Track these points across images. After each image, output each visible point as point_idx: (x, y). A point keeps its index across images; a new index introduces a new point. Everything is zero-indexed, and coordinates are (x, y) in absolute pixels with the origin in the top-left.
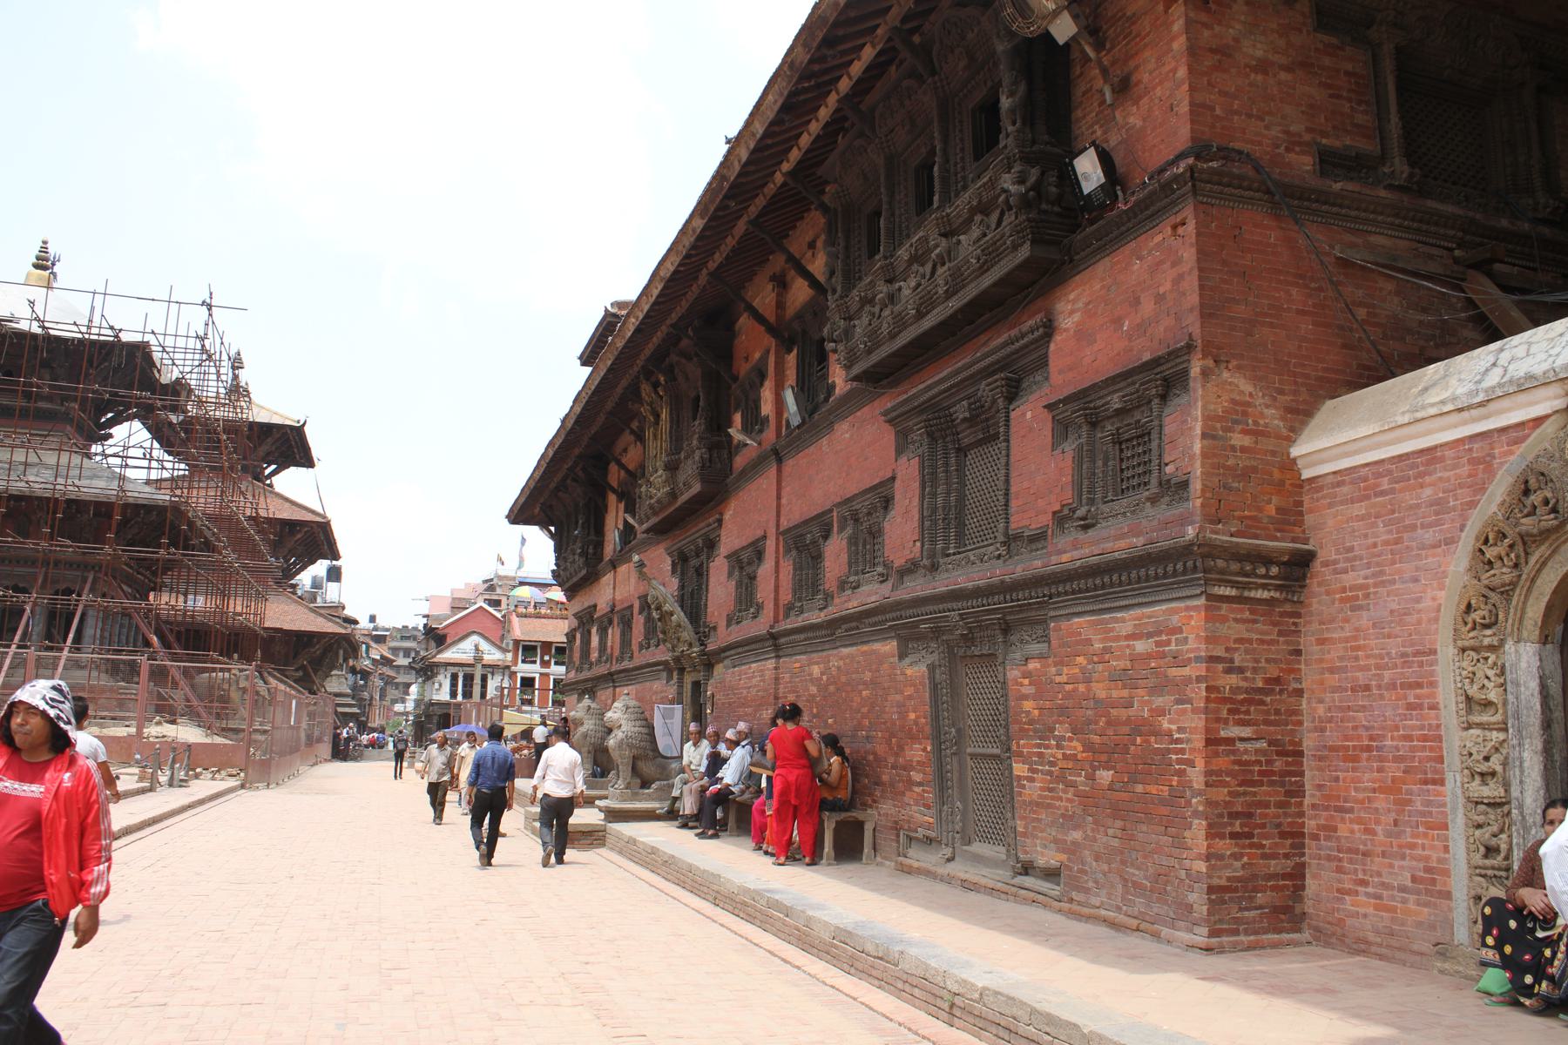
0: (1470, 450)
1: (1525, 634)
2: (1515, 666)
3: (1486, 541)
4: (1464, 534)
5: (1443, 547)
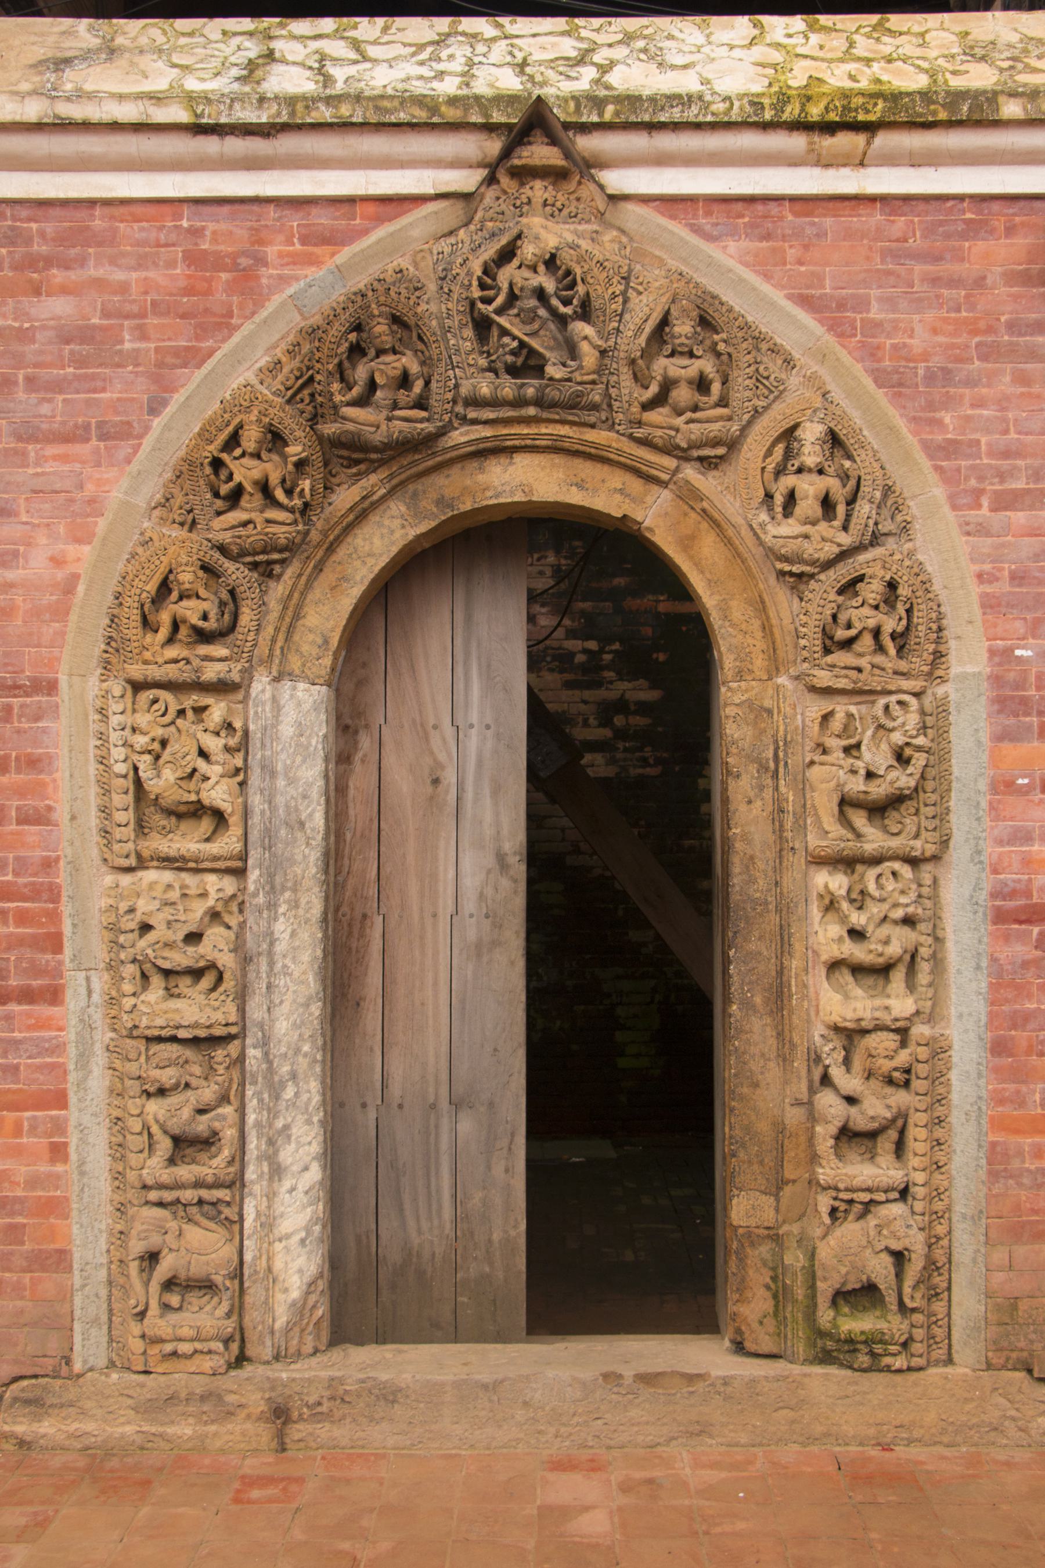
0: (196, 233)
1: (295, 663)
2: (271, 730)
3: (233, 441)
4: (157, 423)
5: (94, 442)
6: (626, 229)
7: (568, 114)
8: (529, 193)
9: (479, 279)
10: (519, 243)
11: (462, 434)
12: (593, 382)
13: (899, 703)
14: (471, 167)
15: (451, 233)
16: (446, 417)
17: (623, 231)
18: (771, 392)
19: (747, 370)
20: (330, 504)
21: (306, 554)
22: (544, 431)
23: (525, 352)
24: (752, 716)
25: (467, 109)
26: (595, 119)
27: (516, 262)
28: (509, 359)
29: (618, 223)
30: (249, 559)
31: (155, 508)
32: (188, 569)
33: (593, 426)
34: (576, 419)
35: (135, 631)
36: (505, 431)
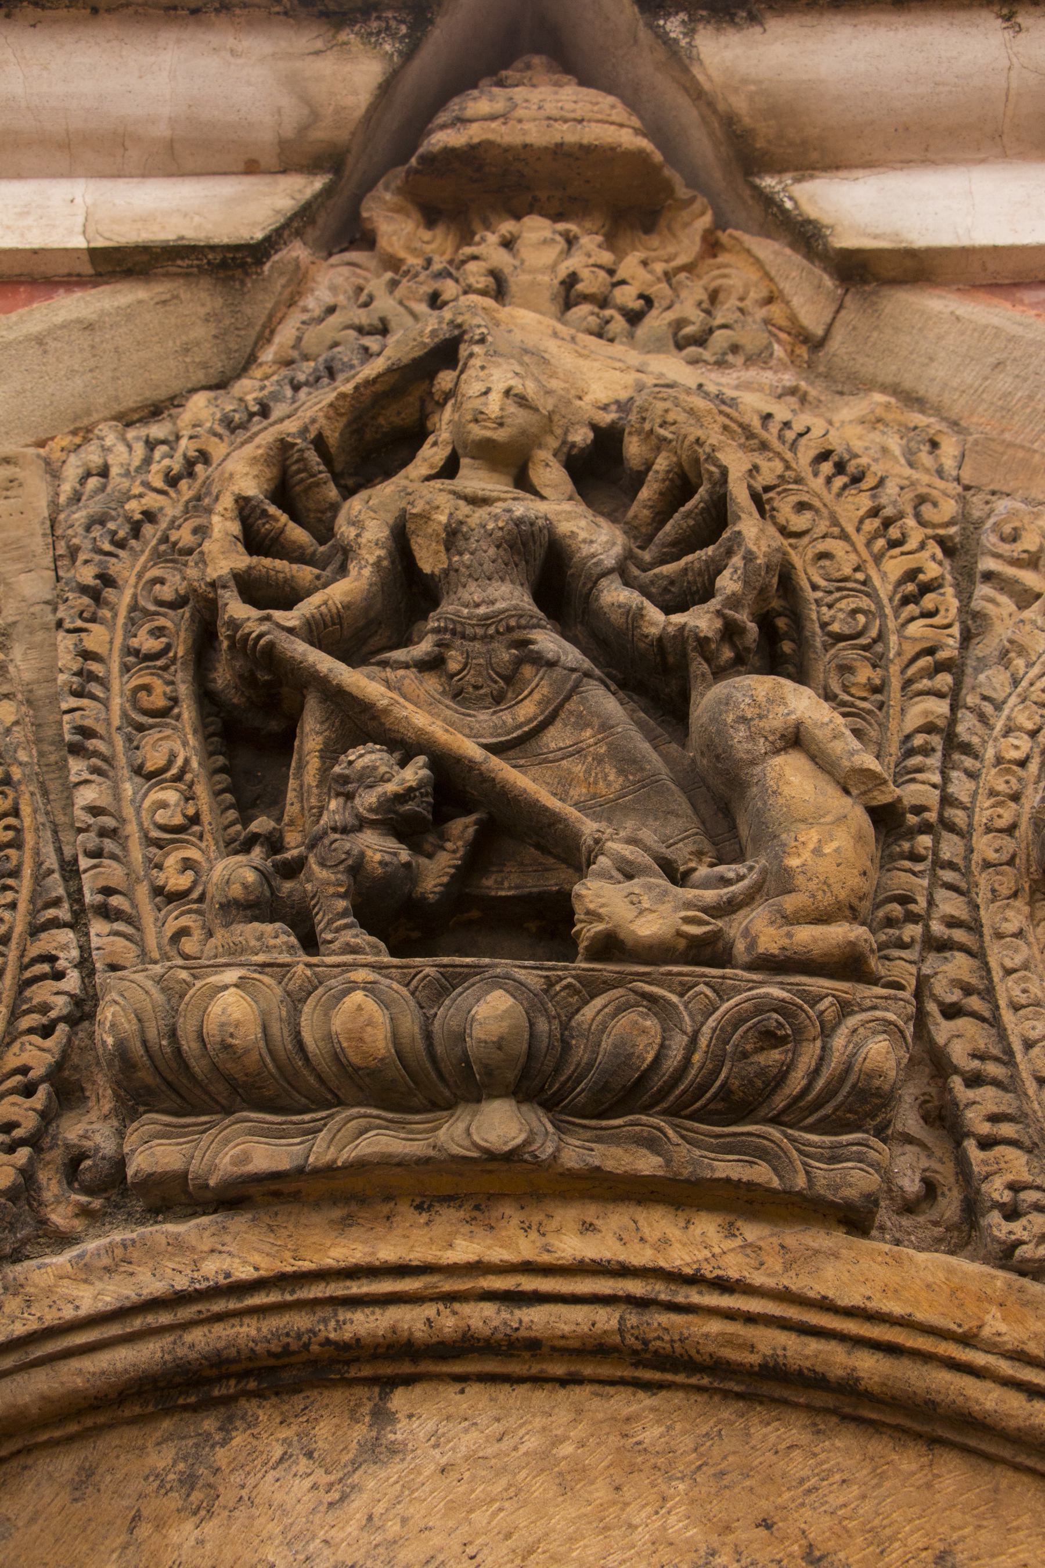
6: (930, 391)
8: (500, 258)
9: (245, 509)
10: (445, 379)
11: (85, 1271)
14: (251, 168)
15: (155, 411)
29: (888, 372)
34: (761, 1173)
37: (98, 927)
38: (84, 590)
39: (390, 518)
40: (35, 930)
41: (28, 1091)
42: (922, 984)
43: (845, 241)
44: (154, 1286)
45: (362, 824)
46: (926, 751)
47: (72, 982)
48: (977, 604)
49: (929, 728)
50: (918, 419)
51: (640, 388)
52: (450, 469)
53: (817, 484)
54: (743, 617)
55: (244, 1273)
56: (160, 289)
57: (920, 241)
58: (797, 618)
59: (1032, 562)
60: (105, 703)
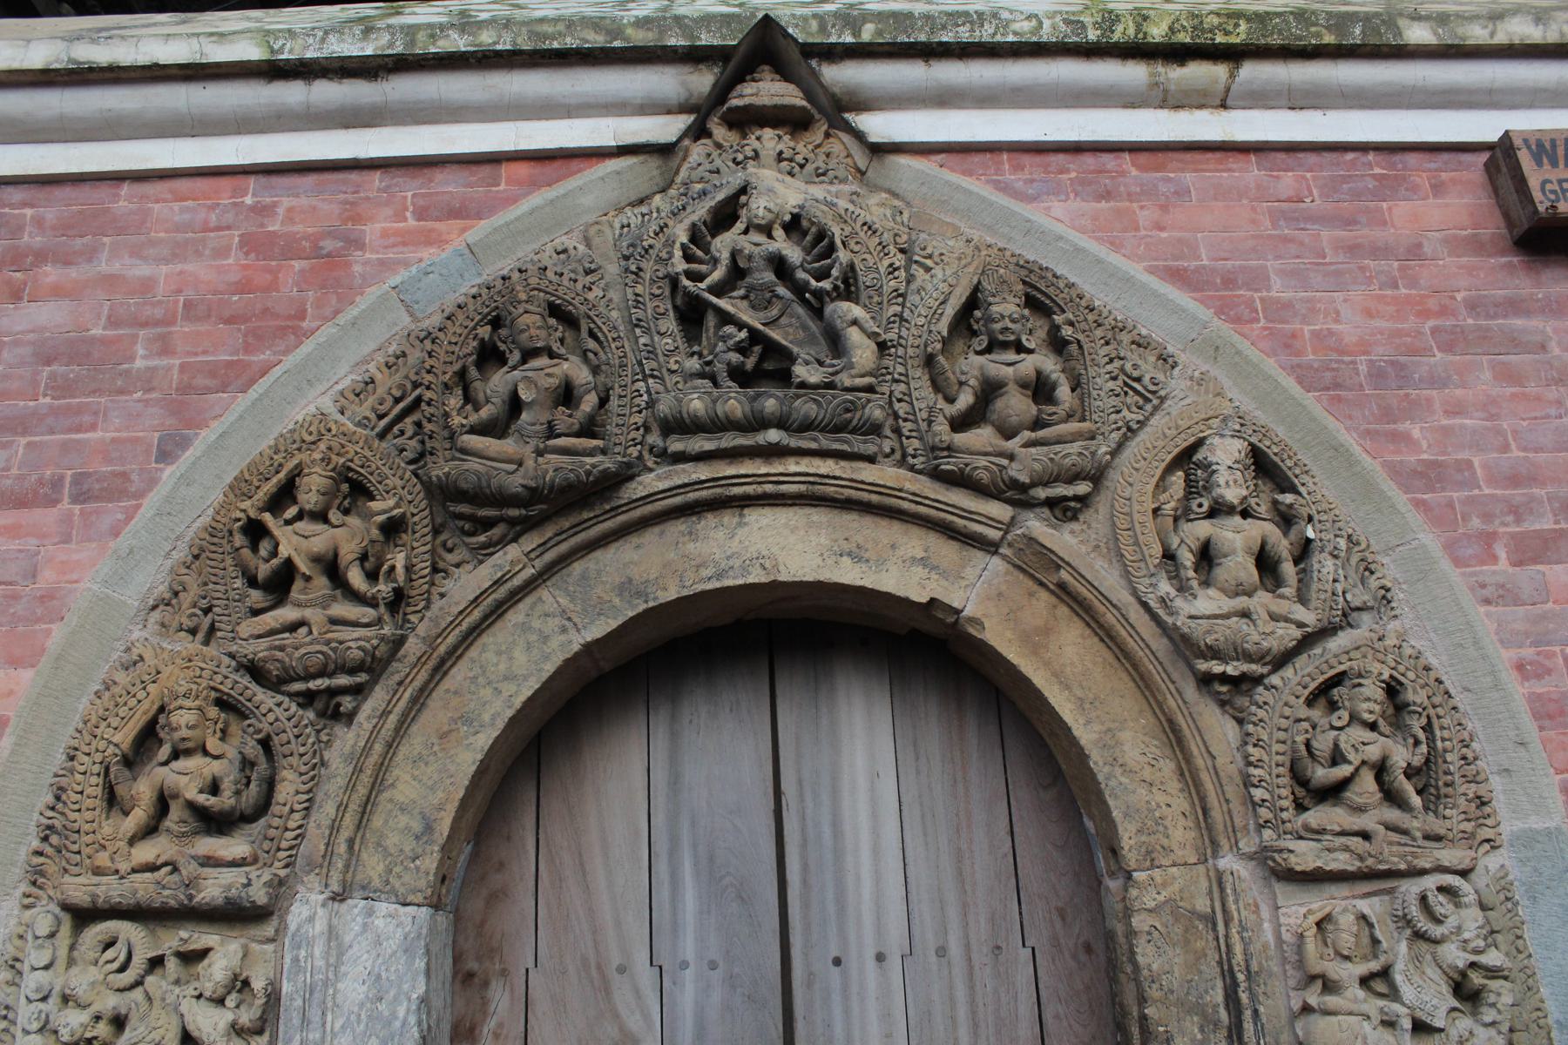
0: (262, 211)
1: (372, 866)
2: (320, 993)
3: (285, 495)
4: (169, 473)
5: (65, 505)
7: (808, 34)
8: (756, 145)
9: (684, 247)
10: (743, 199)
11: (659, 478)
12: (870, 389)
13: (1441, 889)
14: (669, 112)
15: (641, 202)
16: (634, 452)
17: (895, 195)
18: (1147, 400)
19: (1109, 368)
20: (442, 595)
21: (397, 678)
22: (793, 468)
23: (757, 349)
24: (1178, 930)
25: (662, 32)
26: (848, 39)
27: (740, 226)
28: (735, 357)
29: (887, 184)
30: (297, 686)
31: (154, 608)
32: (188, 703)
33: (871, 459)
34: (845, 447)
35: (88, 815)
36: (731, 471)
37: (651, 381)
38: (632, 273)
39: (730, 249)
40: (633, 382)
41: (638, 429)
42: (891, 392)
43: (873, 139)
44: (680, 482)
45: (729, 350)
46: (894, 322)
47: (645, 397)
48: (912, 272)
49: (895, 315)
50: (897, 203)
51: (806, 200)
52: (746, 232)
53: (862, 234)
54: (839, 283)
55: (703, 478)
56: (641, 158)
57: (898, 139)
58: (856, 279)
59: (930, 257)
60: (645, 311)
